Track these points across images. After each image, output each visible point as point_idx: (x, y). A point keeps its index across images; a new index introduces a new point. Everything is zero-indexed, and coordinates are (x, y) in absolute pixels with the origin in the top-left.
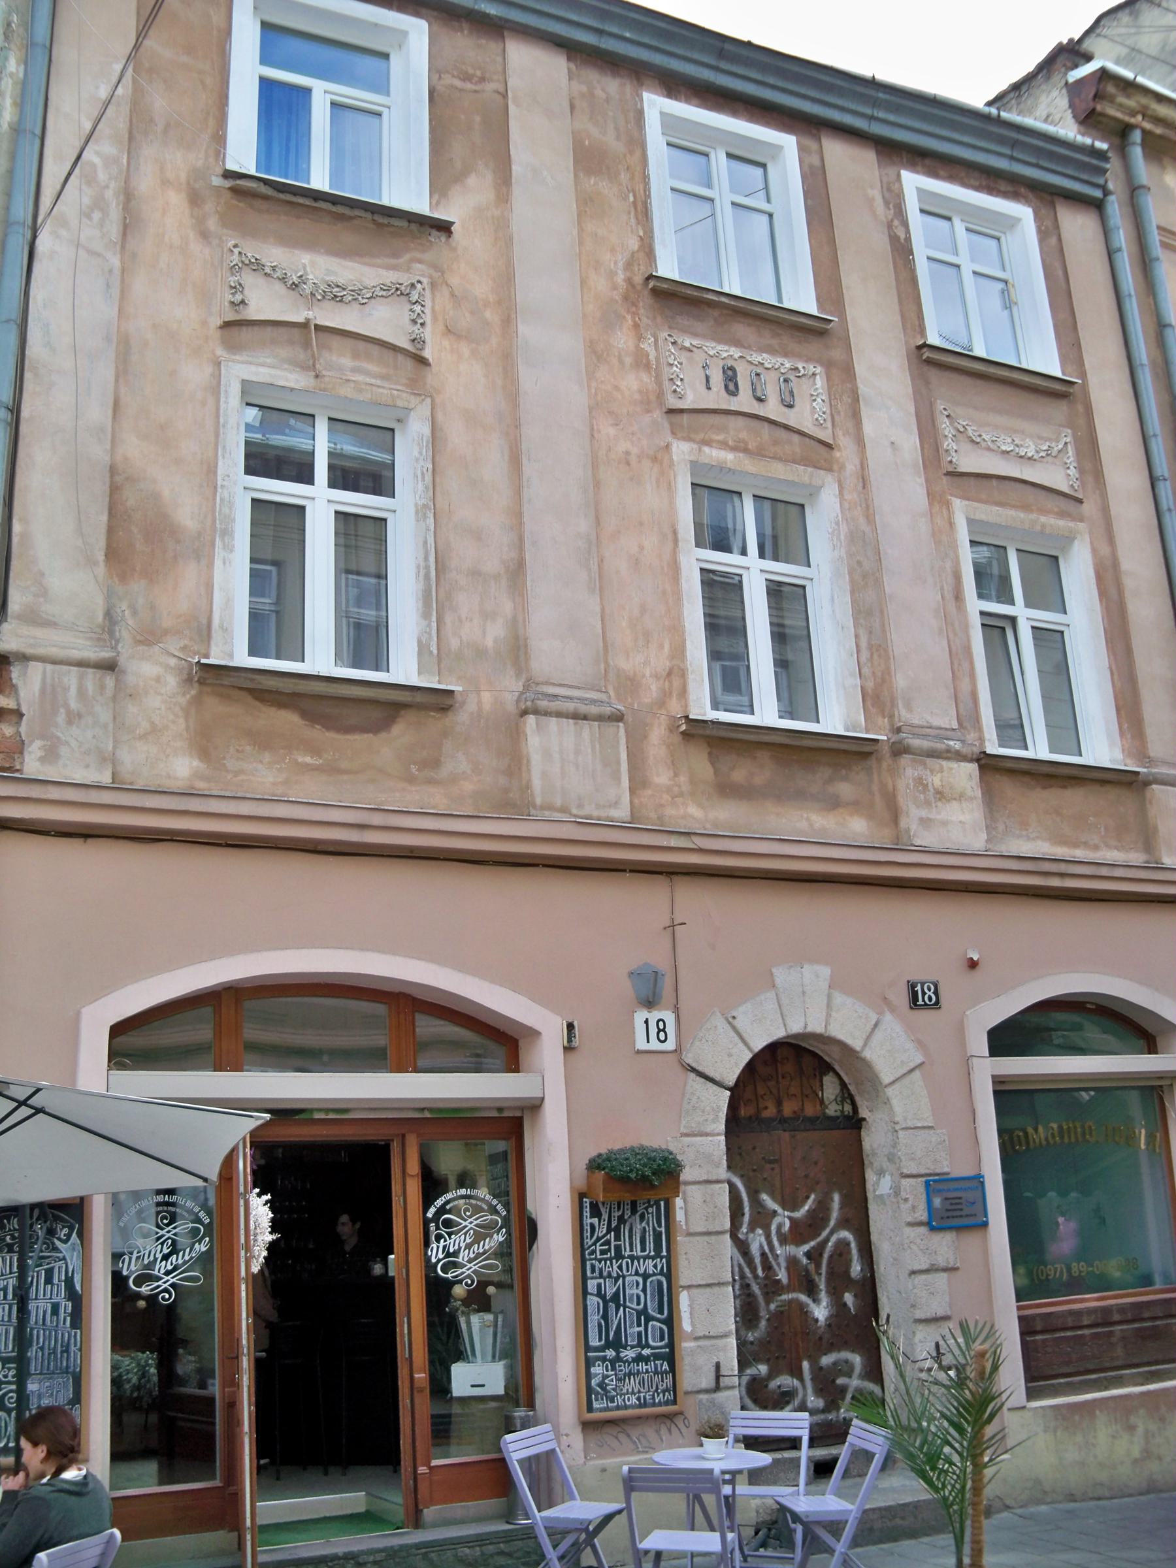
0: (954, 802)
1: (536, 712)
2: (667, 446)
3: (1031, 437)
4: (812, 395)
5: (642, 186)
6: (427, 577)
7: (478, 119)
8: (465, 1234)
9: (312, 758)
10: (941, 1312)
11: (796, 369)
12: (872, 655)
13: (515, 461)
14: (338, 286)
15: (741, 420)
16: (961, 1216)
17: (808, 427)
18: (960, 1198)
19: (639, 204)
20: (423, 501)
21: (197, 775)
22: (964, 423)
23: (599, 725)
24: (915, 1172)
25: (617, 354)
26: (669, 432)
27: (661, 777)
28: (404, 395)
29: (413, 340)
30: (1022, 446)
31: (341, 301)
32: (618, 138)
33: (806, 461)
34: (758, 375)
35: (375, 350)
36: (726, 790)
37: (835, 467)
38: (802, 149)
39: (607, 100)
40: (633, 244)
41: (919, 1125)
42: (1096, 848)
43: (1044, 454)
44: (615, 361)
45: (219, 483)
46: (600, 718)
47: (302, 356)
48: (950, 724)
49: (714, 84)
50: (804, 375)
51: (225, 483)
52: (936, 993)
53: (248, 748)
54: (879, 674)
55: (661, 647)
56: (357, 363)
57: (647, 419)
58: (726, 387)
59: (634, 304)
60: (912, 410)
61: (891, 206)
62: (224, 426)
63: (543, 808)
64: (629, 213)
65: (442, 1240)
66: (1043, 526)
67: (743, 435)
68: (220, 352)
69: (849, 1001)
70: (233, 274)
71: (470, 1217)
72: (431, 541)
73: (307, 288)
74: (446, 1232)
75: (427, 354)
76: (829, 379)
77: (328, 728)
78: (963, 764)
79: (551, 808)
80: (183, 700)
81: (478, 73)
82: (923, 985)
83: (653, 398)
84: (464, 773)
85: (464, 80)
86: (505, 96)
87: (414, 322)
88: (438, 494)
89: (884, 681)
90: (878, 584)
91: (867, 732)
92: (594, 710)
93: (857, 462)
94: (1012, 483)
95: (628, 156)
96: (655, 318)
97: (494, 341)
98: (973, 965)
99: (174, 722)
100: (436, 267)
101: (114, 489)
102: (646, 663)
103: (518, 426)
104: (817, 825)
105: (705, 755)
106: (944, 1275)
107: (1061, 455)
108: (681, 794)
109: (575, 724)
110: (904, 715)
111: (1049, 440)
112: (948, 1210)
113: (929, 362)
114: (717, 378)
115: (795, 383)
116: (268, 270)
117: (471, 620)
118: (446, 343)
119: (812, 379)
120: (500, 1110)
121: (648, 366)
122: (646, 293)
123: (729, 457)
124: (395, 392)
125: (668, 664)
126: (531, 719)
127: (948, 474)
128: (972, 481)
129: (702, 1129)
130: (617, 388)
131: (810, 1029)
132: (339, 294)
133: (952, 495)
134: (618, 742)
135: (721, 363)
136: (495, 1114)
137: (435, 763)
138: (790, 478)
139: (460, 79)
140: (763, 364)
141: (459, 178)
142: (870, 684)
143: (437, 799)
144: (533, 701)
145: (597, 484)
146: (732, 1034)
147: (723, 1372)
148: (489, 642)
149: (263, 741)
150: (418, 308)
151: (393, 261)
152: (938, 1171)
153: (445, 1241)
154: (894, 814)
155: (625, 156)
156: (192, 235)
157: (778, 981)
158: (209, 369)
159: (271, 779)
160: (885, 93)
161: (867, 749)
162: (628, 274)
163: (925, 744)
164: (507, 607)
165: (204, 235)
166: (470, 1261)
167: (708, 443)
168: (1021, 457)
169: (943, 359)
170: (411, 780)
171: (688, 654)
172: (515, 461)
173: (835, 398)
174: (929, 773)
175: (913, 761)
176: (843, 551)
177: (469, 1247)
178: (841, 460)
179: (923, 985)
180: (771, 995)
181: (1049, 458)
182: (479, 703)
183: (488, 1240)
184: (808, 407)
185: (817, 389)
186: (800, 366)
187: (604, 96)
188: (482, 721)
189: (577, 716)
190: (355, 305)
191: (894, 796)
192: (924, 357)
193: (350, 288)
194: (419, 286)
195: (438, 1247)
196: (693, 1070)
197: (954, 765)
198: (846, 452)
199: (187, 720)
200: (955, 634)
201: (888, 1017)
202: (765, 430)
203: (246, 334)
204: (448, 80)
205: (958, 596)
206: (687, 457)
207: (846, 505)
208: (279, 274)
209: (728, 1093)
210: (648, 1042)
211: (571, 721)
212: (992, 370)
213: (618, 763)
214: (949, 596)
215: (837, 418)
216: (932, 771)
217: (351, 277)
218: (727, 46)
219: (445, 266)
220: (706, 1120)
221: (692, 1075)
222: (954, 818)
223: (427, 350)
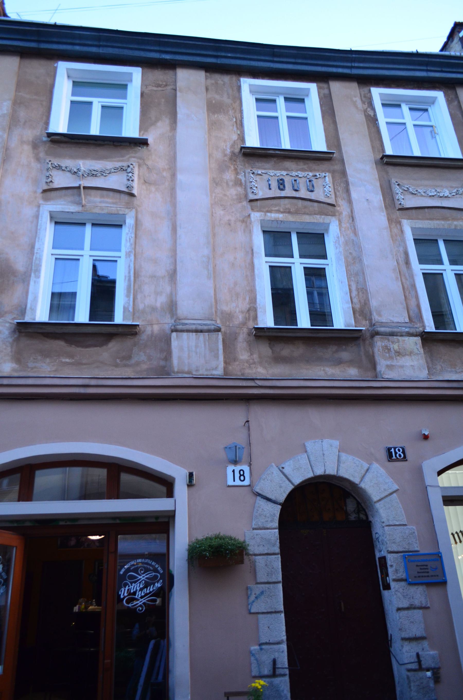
0: (407, 356)
1: (176, 331)
2: (249, 216)
3: (446, 187)
4: (324, 185)
5: (239, 115)
6: (129, 280)
7: (163, 100)
8: (140, 583)
9: (69, 359)
10: (419, 634)
11: (316, 176)
12: (359, 293)
13: (174, 229)
14: (95, 171)
15: (287, 201)
16: (428, 576)
17: (322, 199)
18: (427, 566)
19: (238, 122)
20: (130, 250)
21: (14, 370)
22: (407, 187)
23: (208, 335)
24: (396, 550)
25: (225, 181)
26: (250, 210)
27: (244, 356)
28: (123, 209)
29: (128, 187)
30: (441, 192)
31: (96, 176)
32: (229, 98)
33: (321, 213)
34: (295, 180)
35: (111, 193)
37: (337, 214)
38: (319, 88)
39: (224, 84)
40: (235, 137)
41: (397, 523)
43: (454, 194)
44: (225, 185)
45: (36, 251)
46: (209, 331)
47: (77, 199)
48: (405, 320)
49: (274, 68)
50: (320, 178)
51: (38, 252)
52: (404, 452)
53: (39, 358)
54: (363, 301)
55: (245, 299)
56: (102, 199)
57: (240, 205)
59: (234, 161)
60: (378, 184)
61: (366, 103)
62: (39, 230)
63: (178, 372)
64: (233, 126)
65: (127, 586)
66: (456, 226)
67: (288, 206)
68: (41, 202)
69: (350, 458)
70: (48, 172)
71: (143, 574)
72: (132, 265)
73: (80, 173)
74: (129, 582)
75: (135, 192)
76: (333, 178)
77: (78, 346)
78: (411, 338)
79: (183, 372)
81: (164, 83)
82: (395, 448)
84: (143, 361)
85: (158, 87)
86: (175, 90)
87: (128, 180)
88: (137, 247)
89: (365, 304)
90: (361, 261)
91: (356, 327)
92: (205, 328)
93: (349, 210)
94: (437, 210)
95: (233, 104)
96: (245, 165)
97: (167, 184)
98: (426, 437)
99: (5, 349)
100: (140, 158)
102: (237, 306)
103: (176, 216)
104: (329, 373)
105: (268, 345)
106: (421, 611)
108: (254, 363)
109: (196, 335)
110: (376, 317)
111: (457, 187)
112: (418, 572)
113: (388, 164)
114: (274, 184)
115: (315, 181)
116: (63, 168)
117: (150, 296)
118: (144, 187)
119: (324, 179)
120: (157, 518)
121: (241, 184)
122: (240, 155)
123: (280, 216)
124: (119, 208)
125: (248, 306)
126: (174, 334)
127: (400, 209)
128: (414, 211)
129: (265, 526)
130: (225, 195)
131: (327, 473)
132: (94, 174)
133: (402, 218)
134: (218, 341)
135: (277, 178)
136: (154, 520)
137: (129, 357)
138: (313, 221)
139: (156, 87)
140: (298, 176)
141: (154, 123)
142: (357, 306)
143: (129, 372)
144: (174, 326)
145: (214, 235)
146: (282, 476)
147: (279, 665)
148: (158, 305)
149: (46, 354)
150: (130, 174)
151: (121, 159)
152: (411, 549)
153: (129, 586)
154: (374, 365)
155: (232, 104)
156: (32, 160)
157: (308, 449)
158: (35, 209)
159: (49, 370)
160: (355, 54)
161: (356, 335)
162: (232, 149)
163: (388, 330)
164: (168, 289)
165: (38, 159)
166: (142, 597)
167: (268, 211)
168: (441, 197)
169: (394, 160)
170: (117, 366)
171: (258, 300)
172: (174, 229)
173: (337, 185)
174: (391, 343)
175: (381, 338)
177: (141, 590)
178: (340, 210)
179: (395, 448)
181: (458, 196)
182: (152, 331)
183: (152, 586)
184: (322, 190)
185: (326, 182)
186: (317, 174)
187: (222, 83)
188: (153, 338)
189: (197, 331)
190: (102, 177)
191: (373, 356)
192: (385, 162)
193: (100, 171)
194: (131, 166)
195: (125, 590)
197: (406, 338)
198: (343, 207)
199: (12, 347)
200: (407, 279)
201: (376, 466)
202: (300, 202)
203: (53, 194)
204: (150, 88)
205: (407, 262)
206: (258, 218)
207: (343, 229)
208: (68, 169)
209: (280, 507)
210: (234, 481)
211: (194, 334)
212: (422, 162)
213: (218, 350)
214: (402, 262)
215: (338, 193)
217: (101, 167)
219: (145, 158)
220: (267, 521)
221: (259, 498)
222: (408, 364)
223: (134, 190)
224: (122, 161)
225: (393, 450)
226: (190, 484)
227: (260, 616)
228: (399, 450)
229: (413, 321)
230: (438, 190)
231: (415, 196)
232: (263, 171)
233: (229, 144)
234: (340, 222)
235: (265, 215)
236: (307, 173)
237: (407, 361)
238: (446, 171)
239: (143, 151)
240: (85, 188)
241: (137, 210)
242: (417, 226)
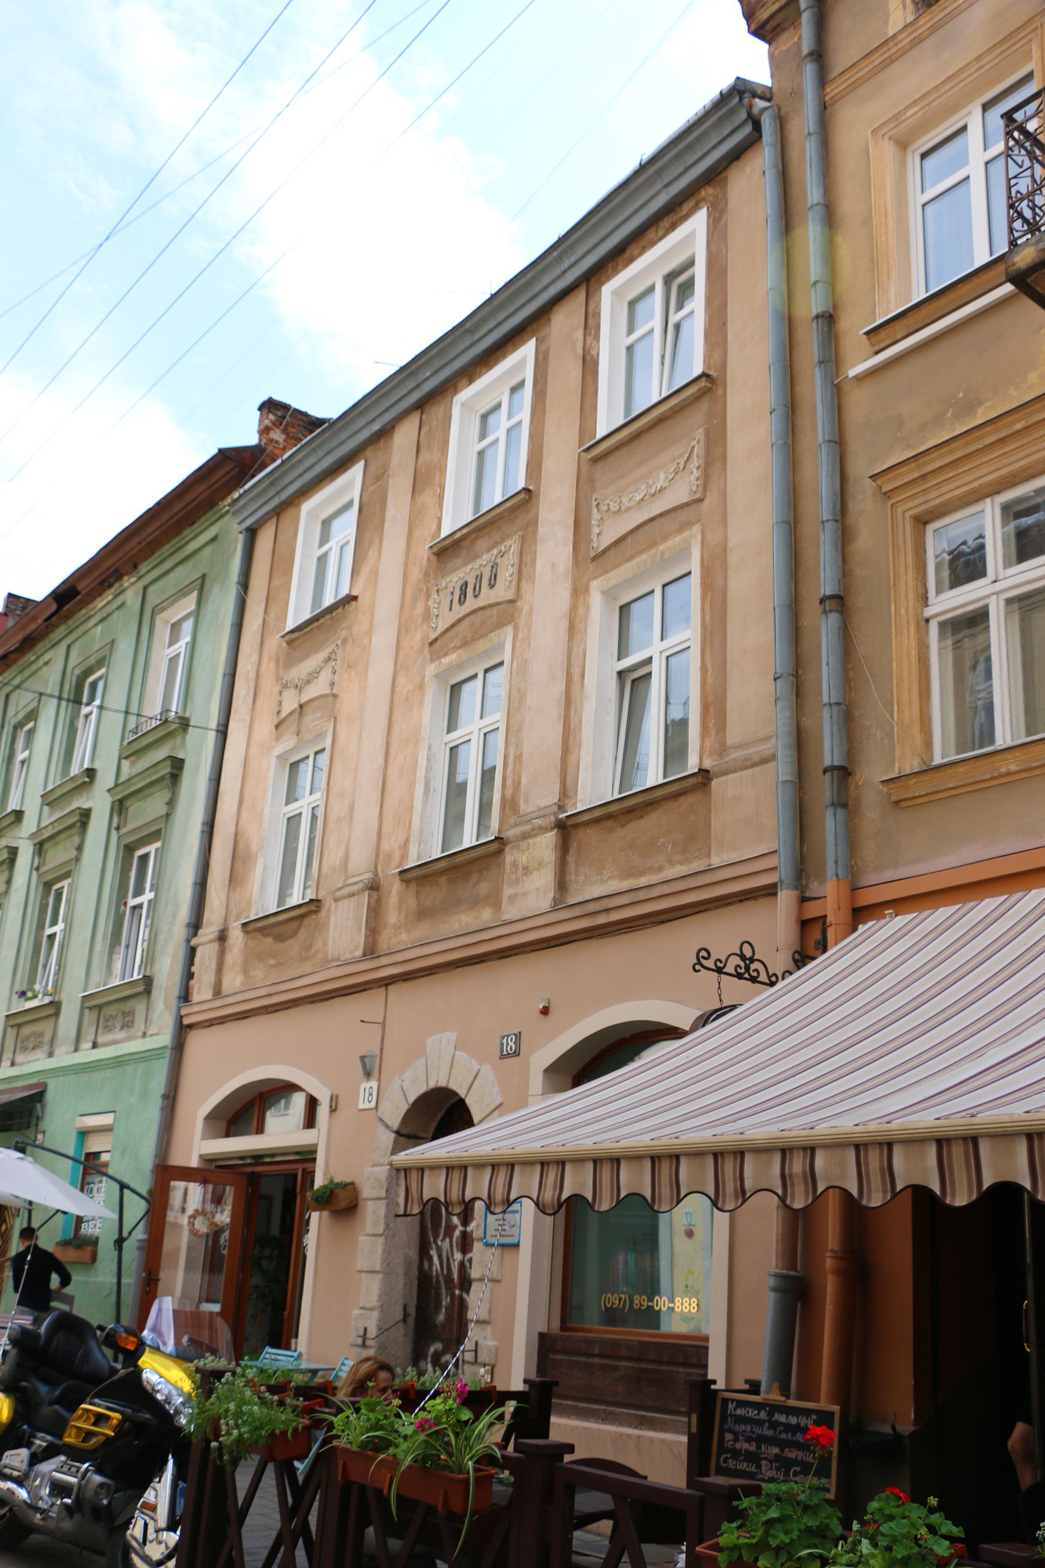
27: (392, 916)
40: (434, 527)
42: (660, 869)
55: (405, 824)
85: (376, 483)
98: (545, 1011)
101: (236, 843)
108: (400, 927)
148: (338, 862)
150: (334, 663)
167: (446, 654)
168: (653, 495)
180: (422, 1061)
181: (678, 476)
196: (381, 1120)
197: (538, 839)
215: (524, 571)
218: (468, 325)
225: (505, 1041)
226: (333, 1110)
227: (364, 1275)
228: (511, 1040)
234: (516, 630)
235: (440, 663)
241: (335, 718)
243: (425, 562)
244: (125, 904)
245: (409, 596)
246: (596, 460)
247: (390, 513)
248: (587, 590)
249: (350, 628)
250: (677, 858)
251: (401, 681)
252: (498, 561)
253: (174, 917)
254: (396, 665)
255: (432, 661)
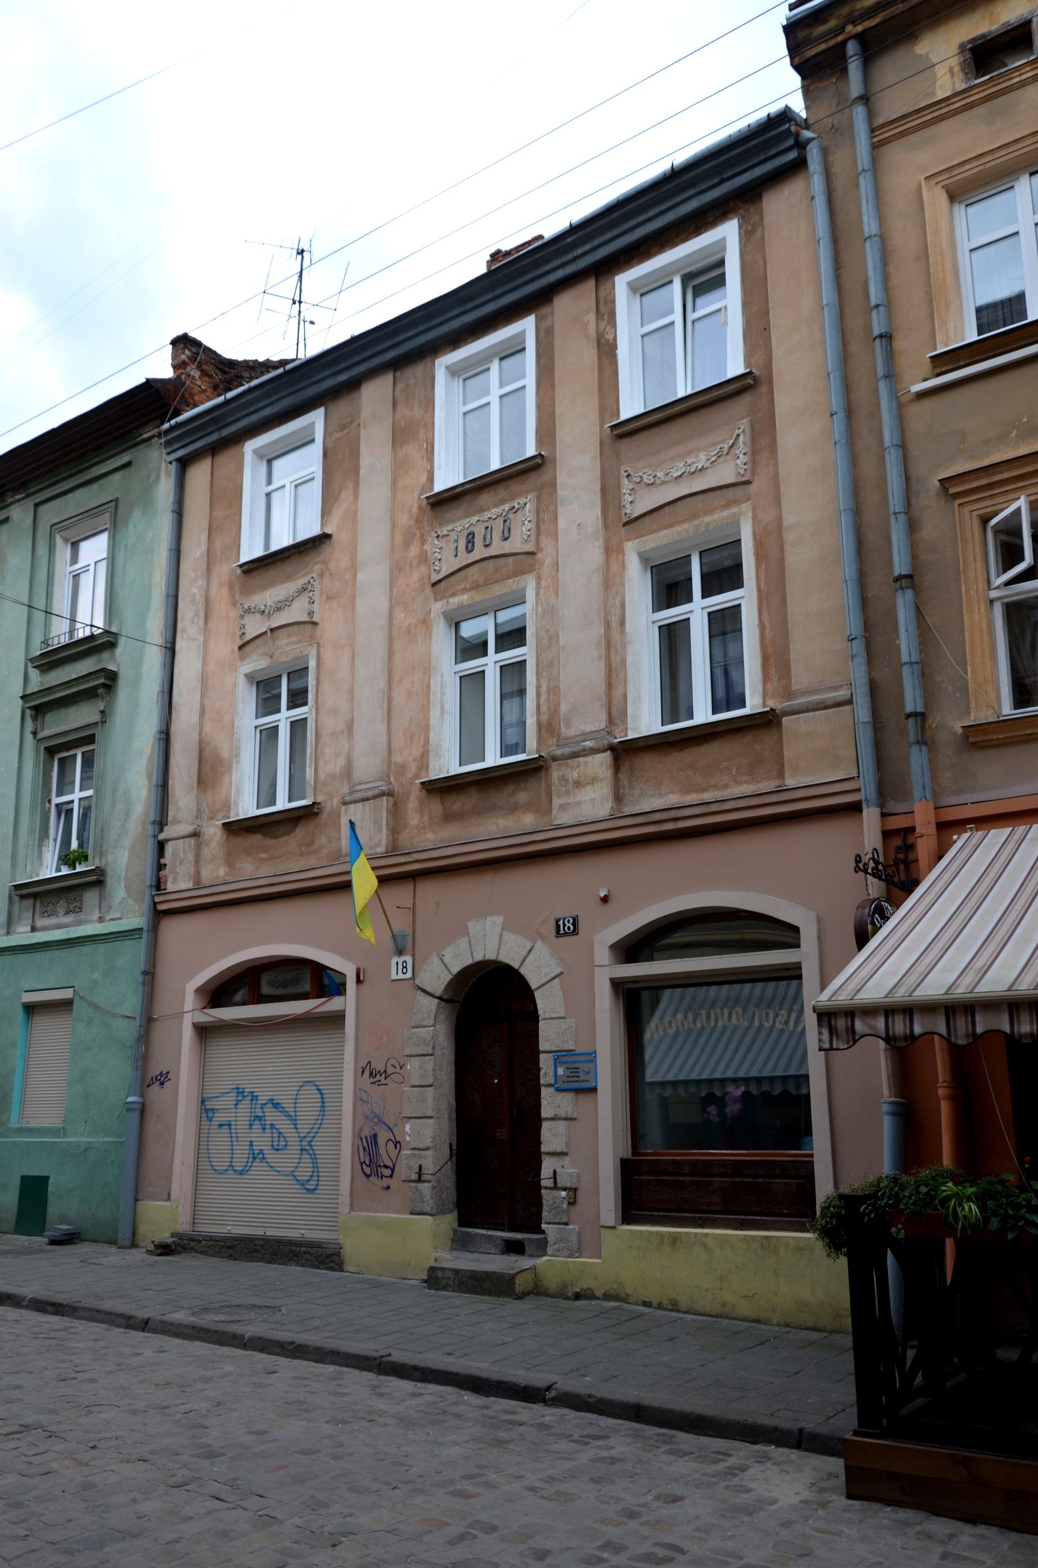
1: (345, 803)
7: (347, 451)
11: (514, 507)
12: (549, 695)
13: (353, 660)
15: (476, 567)
27: (413, 819)
35: (296, 628)
36: (449, 818)
37: (537, 566)
40: (423, 478)
42: (726, 786)
46: (375, 797)
50: (518, 509)
53: (244, 857)
55: (420, 740)
58: (467, 548)
68: (239, 664)
77: (271, 838)
78: (598, 755)
80: (222, 841)
83: (426, 580)
92: (370, 794)
93: (554, 554)
101: (201, 751)
104: (501, 826)
107: (732, 450)
108: (424, 828)
116: (253, 610)
118: (327, 606)
122: (429, 507)
126: (343, 807)
127: (625, 524)
130: (408, 585)
137: (312, 843)
138: (504, 591)
142: (545, 718)
143: (312, 861)
148: (337, 770)
149: (248, 852)
150: (311, 594)
151: (305, 571)
165: (234, 604)
167: (453, 595)
169: (625, 429)
170: (302, 854)
176: (534, 627)
182: (332, 805)
190: (287, 608)
197: (589, 759)
215: (542, 527)
216: (572, 769)
224: (306, 575)
229: (616, 722)
230: (689, 461)
231: (651, 487)
232: (450, 528)
233: (416, 494)
234: (539, 579)
236: (502, 508)
237: (587, 794)
238: (714, 409)
239: (326, 550)
240: (272, 630)
242: (647, 548)
243: (415, 510)
244: (50, 802)
245: (399, 539)
246: (621, 436)
247: (365, 461)
248: (620, 550)
249: (325, 563)
250: (744, 778)
251: (400, 615)
252: (511, 516)
253: (127, 815)
254: (391, 600)
255: (436, 599)
